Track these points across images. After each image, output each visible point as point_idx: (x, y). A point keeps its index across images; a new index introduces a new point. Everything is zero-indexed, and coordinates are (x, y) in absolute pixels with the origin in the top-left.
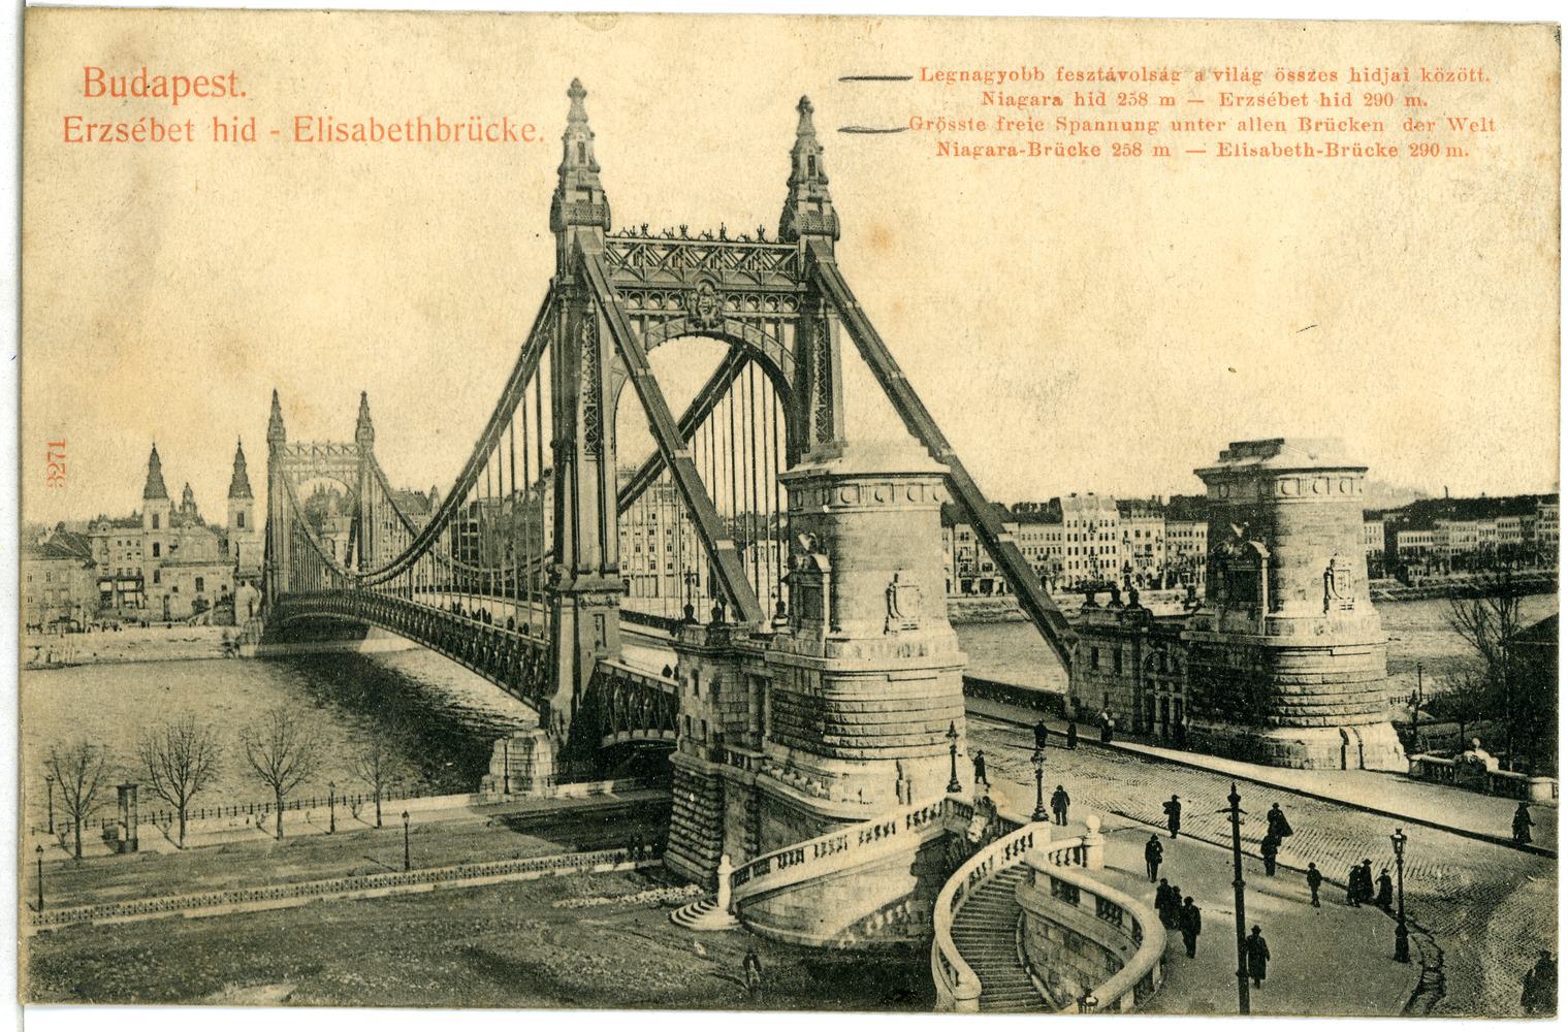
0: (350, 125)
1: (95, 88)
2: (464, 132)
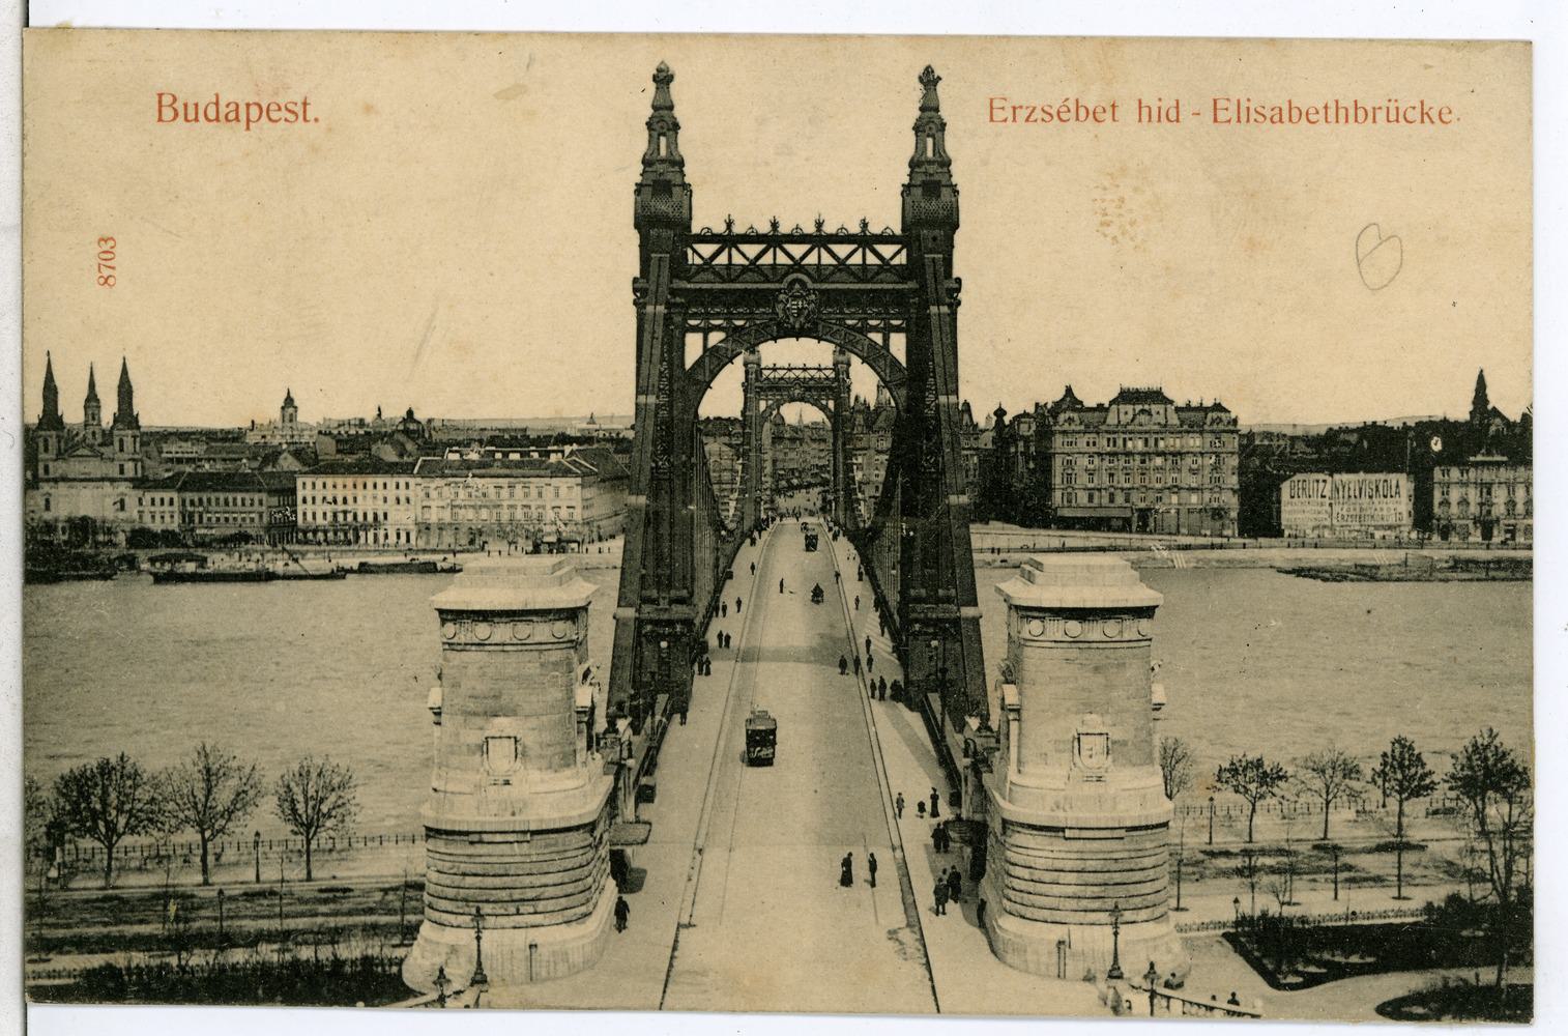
2: (1381, 115)
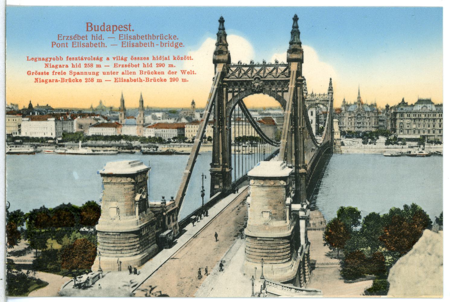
0: (132, 36)
1: (90, 29)
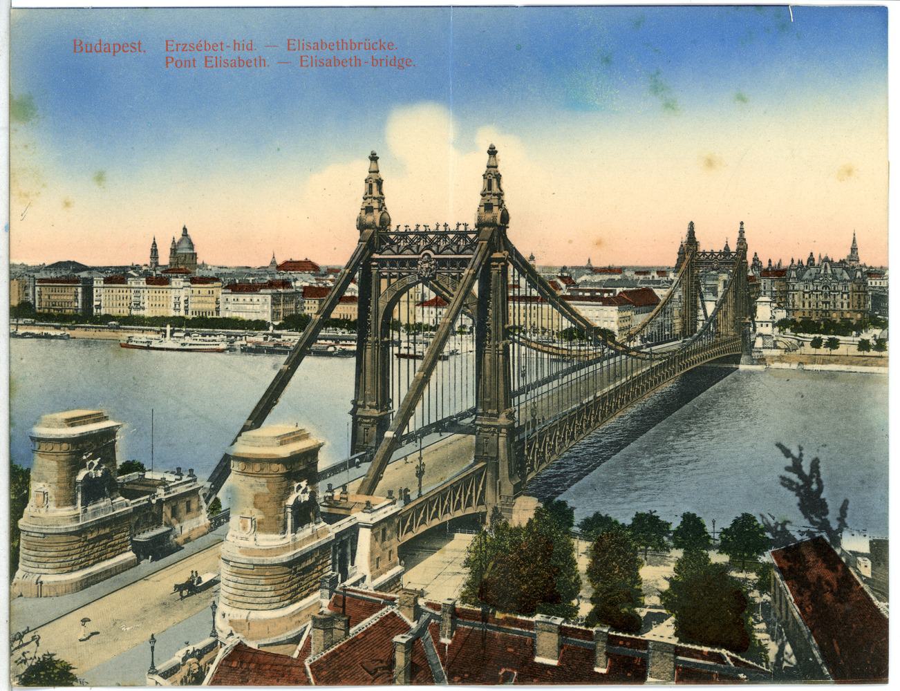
1: (78, 49)
